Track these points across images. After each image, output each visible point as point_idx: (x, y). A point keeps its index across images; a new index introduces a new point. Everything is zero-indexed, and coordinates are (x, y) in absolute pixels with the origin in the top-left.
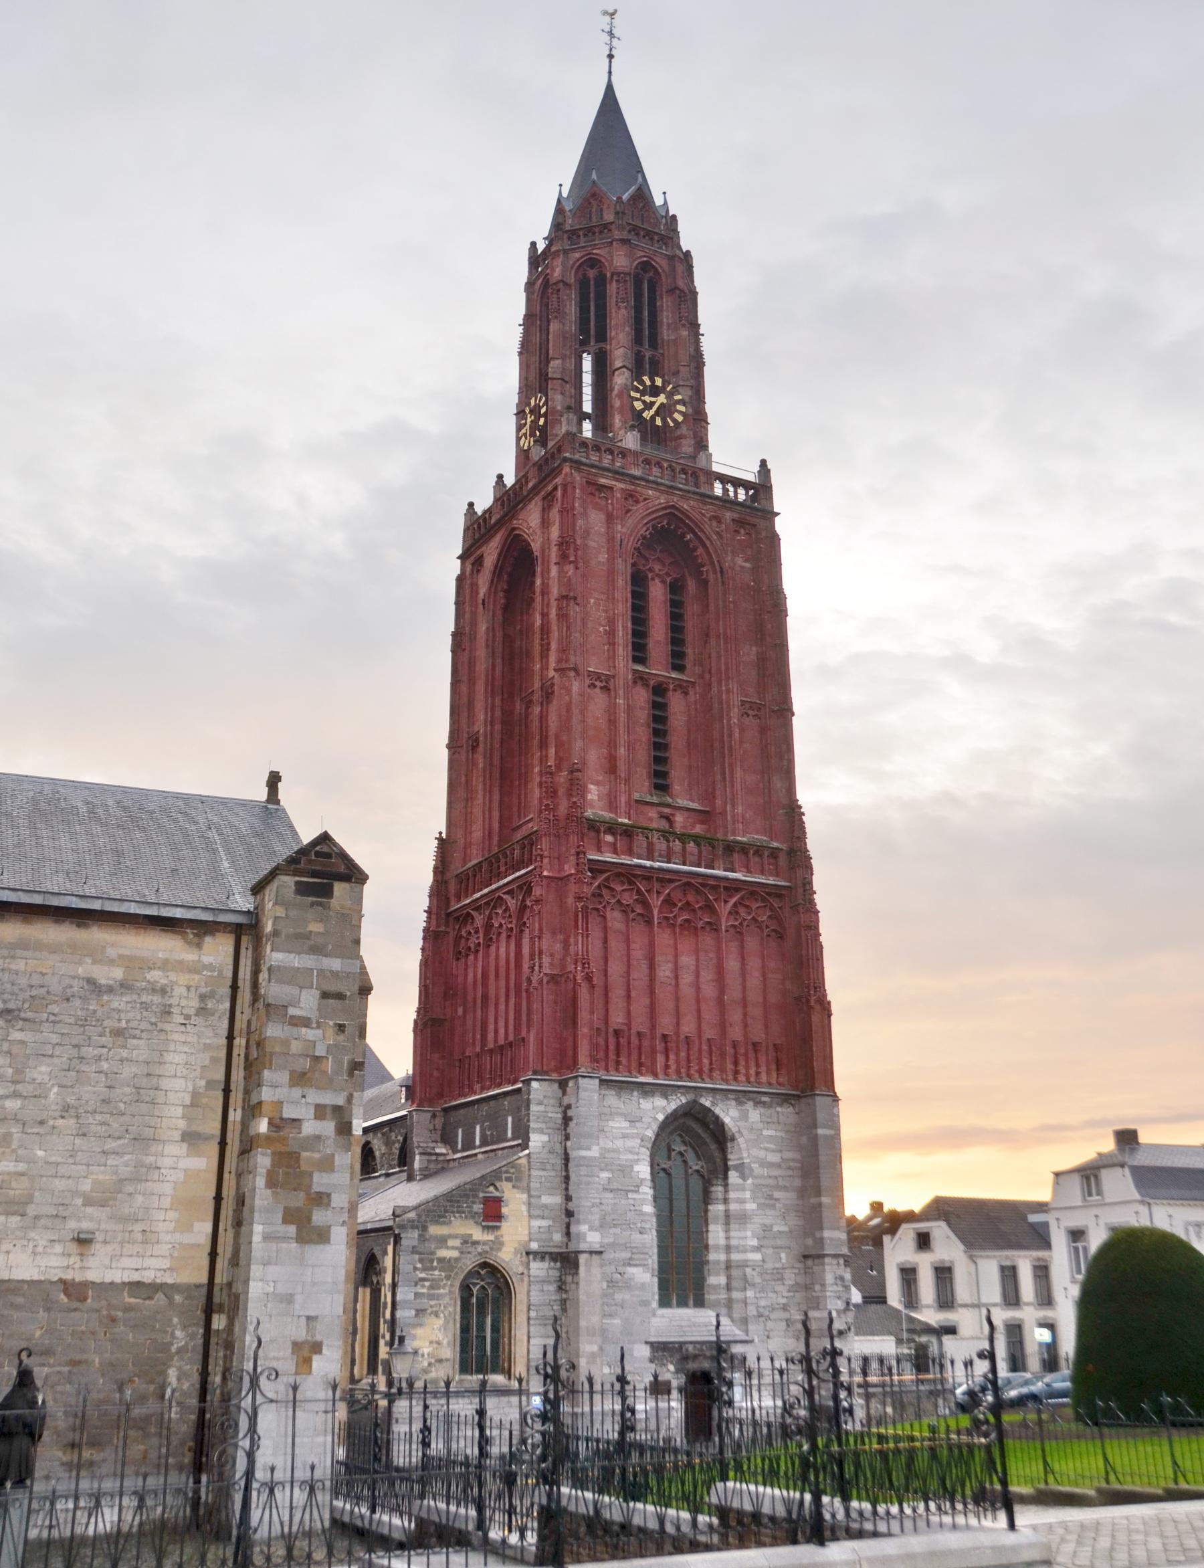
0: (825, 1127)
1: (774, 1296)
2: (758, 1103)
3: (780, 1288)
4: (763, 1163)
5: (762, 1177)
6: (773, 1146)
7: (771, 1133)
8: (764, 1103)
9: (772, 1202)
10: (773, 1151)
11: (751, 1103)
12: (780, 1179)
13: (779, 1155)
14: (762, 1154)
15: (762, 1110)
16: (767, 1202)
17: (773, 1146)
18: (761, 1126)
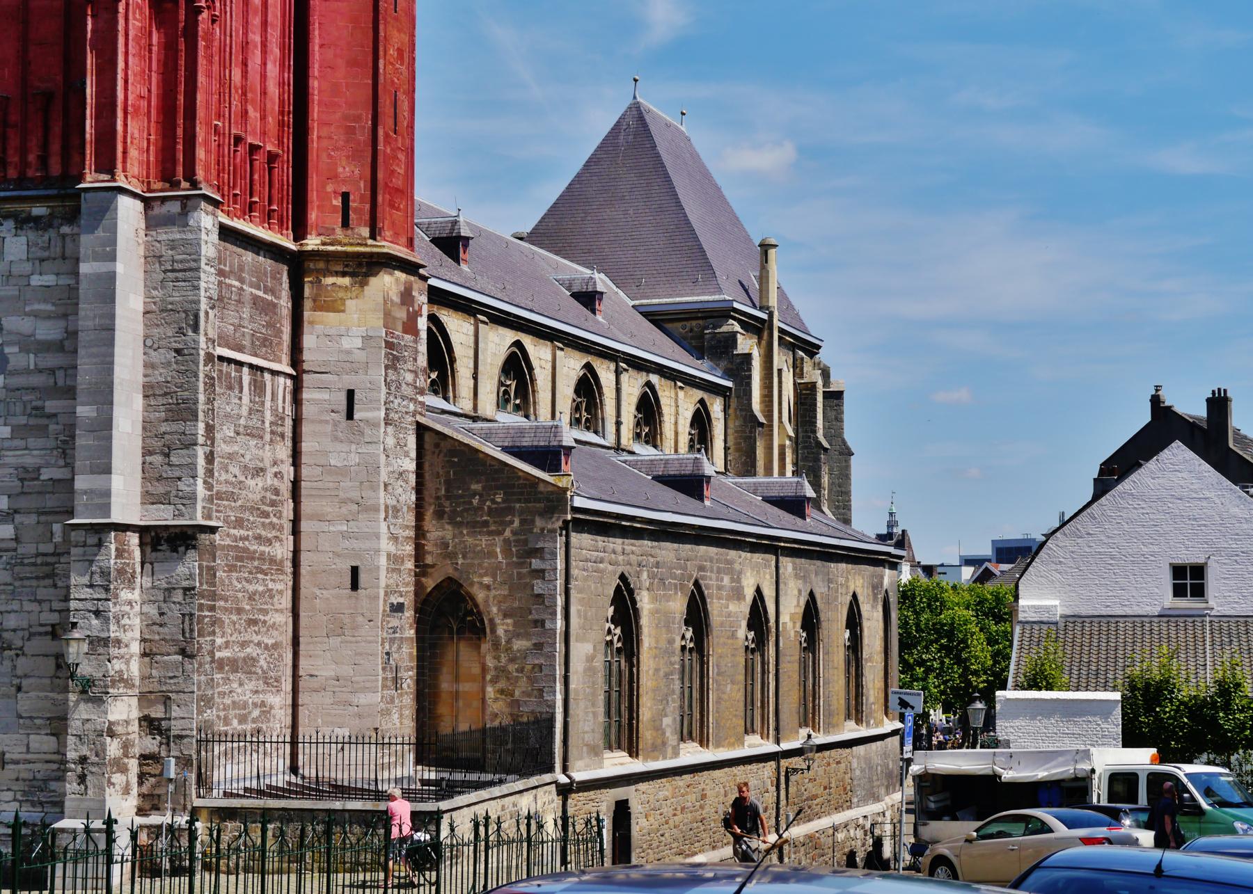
0: (97, 257)
1: (34, 607)
2: (24, 222)
3: (42, 593)
4: (28, 344)
5: (27, 371)
6: (49, 307)
7: (49, 279)
8: (37, 220)
9: (44, 421)
10: (48, 317)
11: (10, 224)
12: (60, 374)
13: (62, 323)
14: (24, 325)
15: (32, 235)
16: (33, 421)
17: (49, 307)
18: (28, 267)
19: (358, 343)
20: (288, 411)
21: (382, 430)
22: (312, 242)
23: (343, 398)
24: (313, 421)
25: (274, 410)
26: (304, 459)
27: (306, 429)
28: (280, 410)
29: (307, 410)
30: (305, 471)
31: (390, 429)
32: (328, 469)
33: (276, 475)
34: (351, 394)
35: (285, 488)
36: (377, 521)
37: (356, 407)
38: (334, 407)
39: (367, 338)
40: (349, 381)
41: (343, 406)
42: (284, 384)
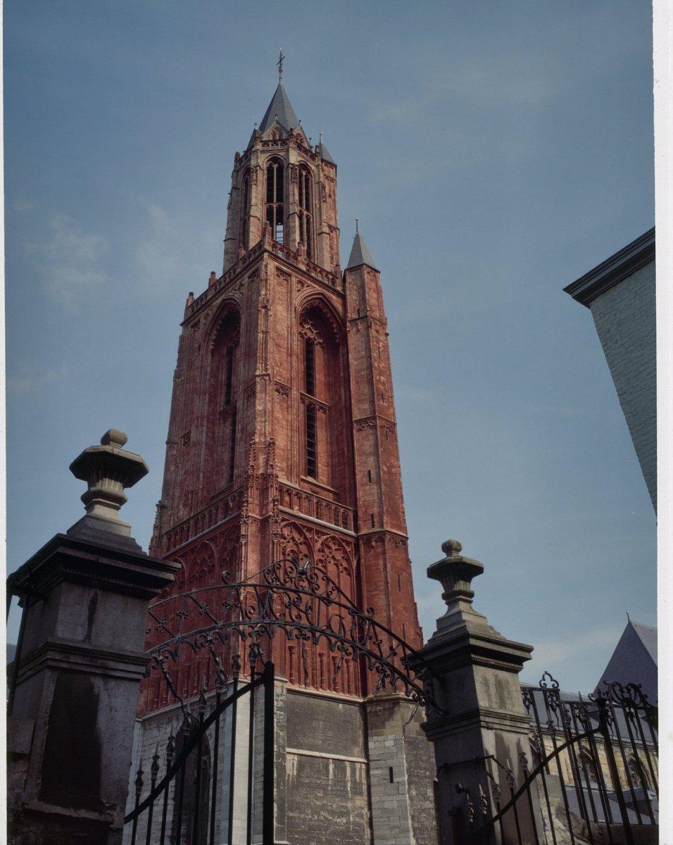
19: (392, 743)
20: (364, 781)
21: (407, 787)
22: (371, 696)
23: (388, 772)
24: (376, 785)
25: (354, 782)
26: (373, 806)
27: (373, 790)
28: (358, 781)
29: (374, 781)
30: (374, 813)
31: (412, 786)
32: (385, 811)
33: (357, 815)
34: (391, 769)
35: (365, 821)
36: (409, 837)
37: (394, 776)
38: (384, 777)
39: (395, 740)
40: (390, 763)
41: (388, 777)
42: (364, 766)
